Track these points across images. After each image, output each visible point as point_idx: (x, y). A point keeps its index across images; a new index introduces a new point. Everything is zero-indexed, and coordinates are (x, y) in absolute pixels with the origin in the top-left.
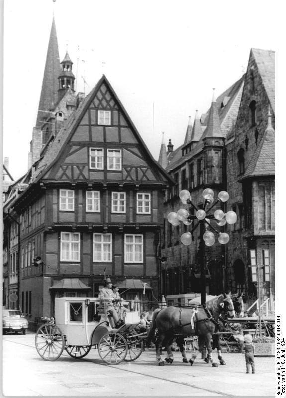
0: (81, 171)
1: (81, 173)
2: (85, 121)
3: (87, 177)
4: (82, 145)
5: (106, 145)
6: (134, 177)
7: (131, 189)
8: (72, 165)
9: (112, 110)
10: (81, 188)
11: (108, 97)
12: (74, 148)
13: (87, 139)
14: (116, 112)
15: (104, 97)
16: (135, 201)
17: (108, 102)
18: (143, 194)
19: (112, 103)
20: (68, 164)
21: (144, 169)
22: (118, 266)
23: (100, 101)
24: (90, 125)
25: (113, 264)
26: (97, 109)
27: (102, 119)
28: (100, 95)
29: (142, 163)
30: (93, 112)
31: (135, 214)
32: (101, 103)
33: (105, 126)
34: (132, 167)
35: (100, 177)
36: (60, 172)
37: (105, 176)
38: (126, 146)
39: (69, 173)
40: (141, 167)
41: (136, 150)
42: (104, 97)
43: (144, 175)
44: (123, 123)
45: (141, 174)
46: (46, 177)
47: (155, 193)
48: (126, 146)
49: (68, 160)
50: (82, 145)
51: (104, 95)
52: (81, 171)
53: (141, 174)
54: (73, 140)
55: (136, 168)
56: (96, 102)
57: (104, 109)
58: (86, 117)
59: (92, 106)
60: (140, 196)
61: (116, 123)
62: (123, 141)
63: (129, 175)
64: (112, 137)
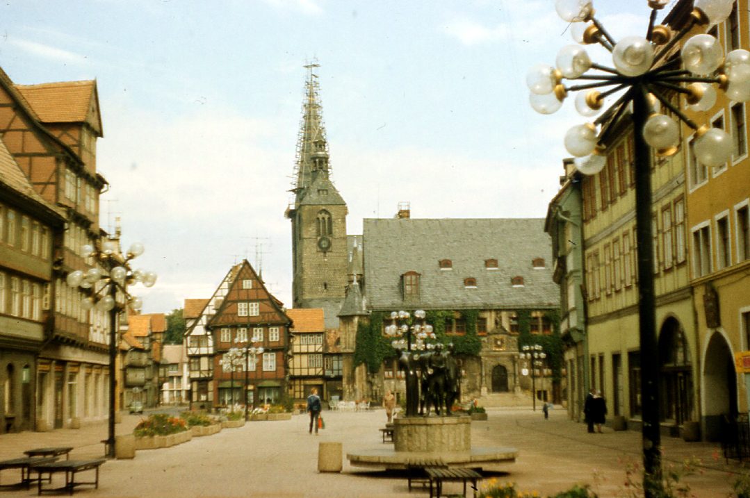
5: (249, 301)
7: (266, 326)
8: (228, 314)
9: (252, 279)
10: (235, 327)
11: (250, 271)
12: (229, 304)
16: (268, 333)
19: (252, 275)
22: (259, 373)
25: (256, 372)
26: (242, 279)
27: (246, 285)
29: (273, 310)
31: (269, 342)
33: (248, 290)
35: (245, 321)
36: (221, 319)
37: (248, 320)
38: (261, 300)
40: (271, 313)
41: (268, 302)
47: (282, 327)
49: (226, 311)
51: (247, 271)
53: (271, 317)
55: (268, 313)
57: (248, 279)
64: (253, 295)
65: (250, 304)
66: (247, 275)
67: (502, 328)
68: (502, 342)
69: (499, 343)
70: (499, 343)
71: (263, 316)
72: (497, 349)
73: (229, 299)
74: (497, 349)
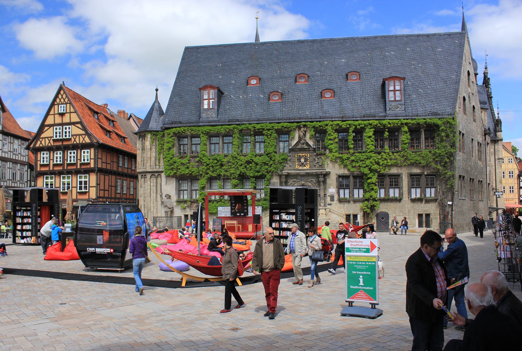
0: (49, 141)
1: (49, 142)
2: (52, 112)
3: (52, 144)
4: (50, 126)
6: (78, 142)
8: (45, 138)
9: (66, 104)
10: (49, 149)
11: (64, 96)
13: (53, 123)
14: (68, 105)
15: (62, 97)
17: (64, 100)
18: (86, 151)
20: (43, 138)
21: (83, 136)
23: (60, 101)
24: (54, 114)
26: (58, 104)
28: (60, 96)
30: (56, 107)
32: (60, 101)
34: (76, 135)
36: (39, 142)
38: (74, 124)
39: (43, 142)
40: (81, 135)
41: (79, 125)
42: (62, 97)
43: (84, 139)
44: (72, 110)
45: (81, 139)
46: (32, 146)
47: (92, 150)
48: (74, 124)
49: (43, 136)
50: (50, 126)
51: (62, 96)
52: (49, 142)
53: (81, 139)
54: (46, 123)
55: (79, 135)
56: (58, 100)
58: (53, 110)
59: (56, 103)
60: (84, 152)
61: (68, 111)
62: (72, 121)
63: (75, 140)
64: (66, 119)
65: (64, 127)
66: (62, 100)
67: (307, 144)
68: (306, 160)
69: (303, 160)
70: (303, 160)
71: (75, 139)
72: (300, 168)
73: (47, 123)
74: (300, 168)
